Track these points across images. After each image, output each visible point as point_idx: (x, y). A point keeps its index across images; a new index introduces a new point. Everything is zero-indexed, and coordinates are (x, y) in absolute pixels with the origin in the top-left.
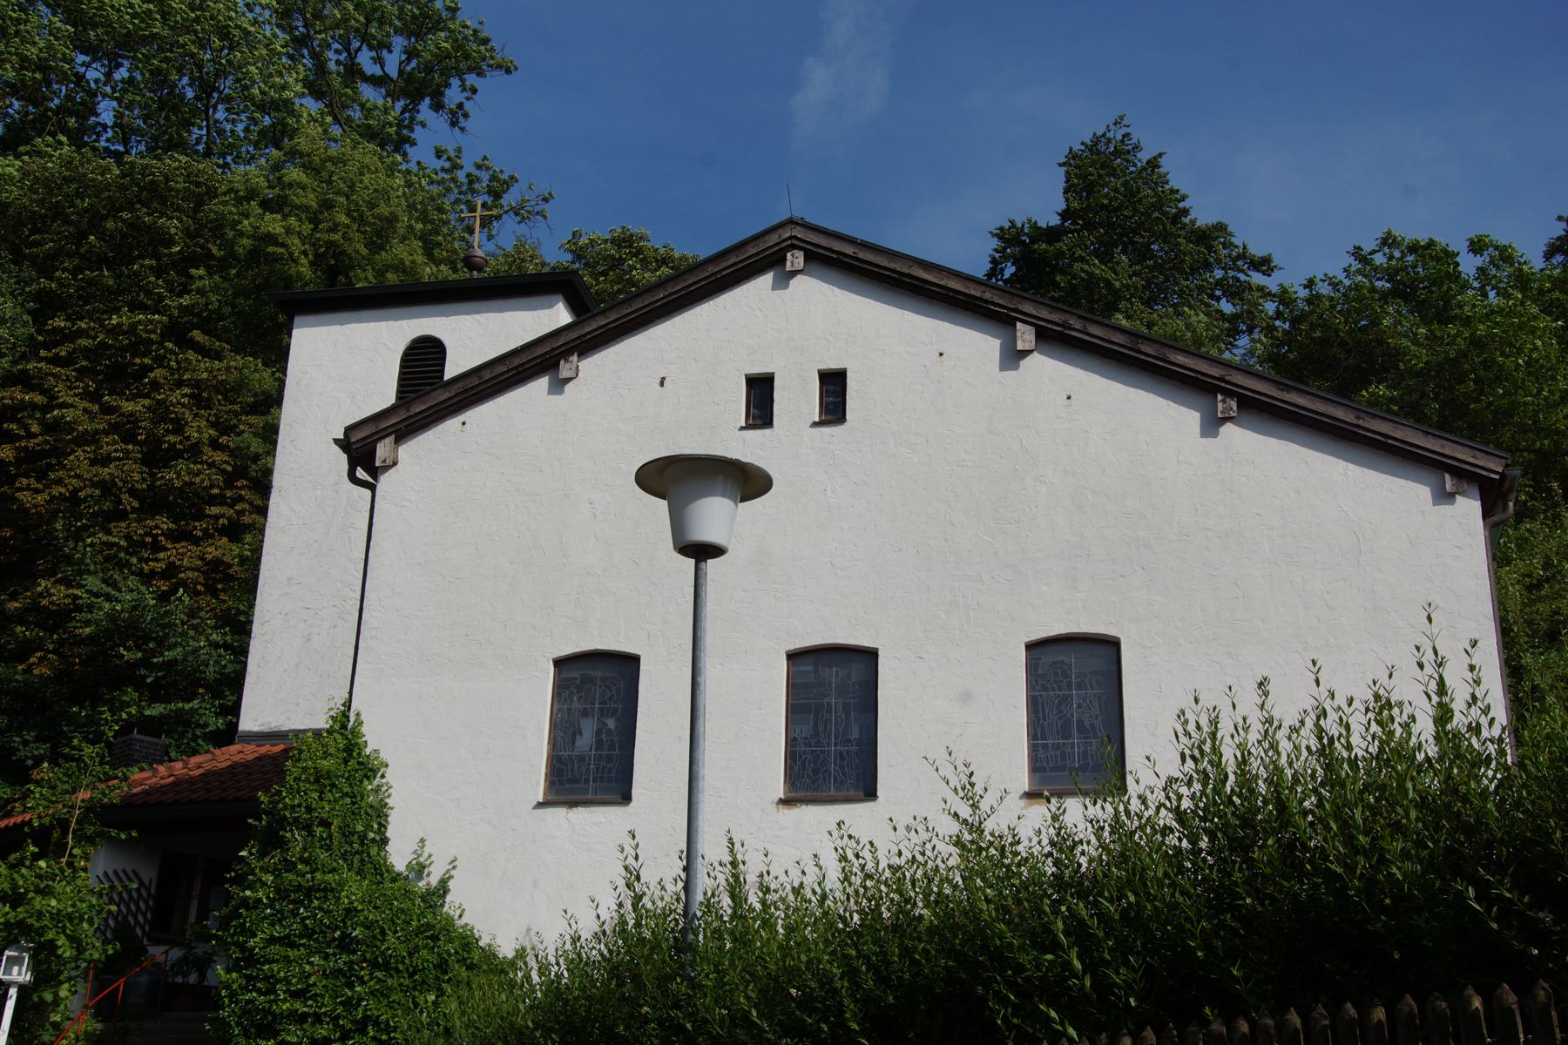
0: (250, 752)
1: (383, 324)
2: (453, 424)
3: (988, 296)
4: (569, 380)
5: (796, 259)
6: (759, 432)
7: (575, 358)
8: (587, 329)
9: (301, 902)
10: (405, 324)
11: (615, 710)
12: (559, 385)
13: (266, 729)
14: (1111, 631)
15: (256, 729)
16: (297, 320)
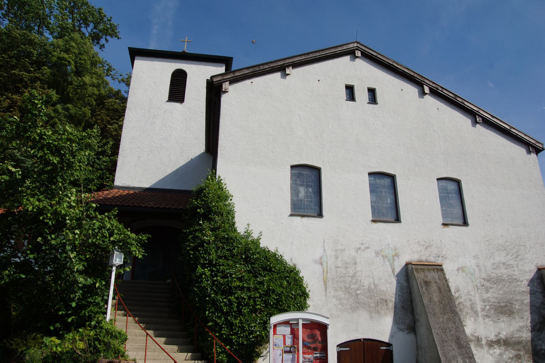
0: (114, 192)
1: (166, 63)
2: (248, 82)
3: (415, 76)
4: (289, 74)
5: (358, 54)
6: (352, 102)
7: (291, 68)
8: (295, 60)
9: (225, 243)
10: (173, 64)
11: (311, 185)
12: (285, 75)
13: (124, 185)
14: (459, 178)
15: (121, 185)
16: (136, 58)
